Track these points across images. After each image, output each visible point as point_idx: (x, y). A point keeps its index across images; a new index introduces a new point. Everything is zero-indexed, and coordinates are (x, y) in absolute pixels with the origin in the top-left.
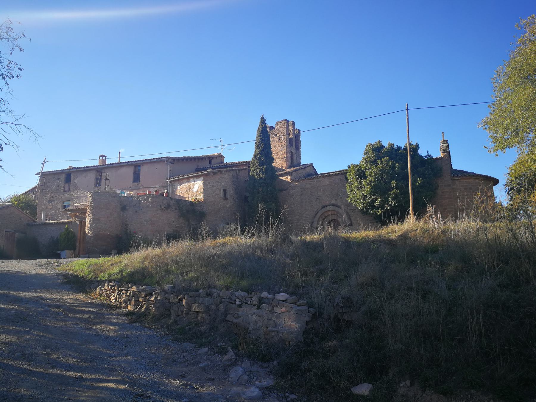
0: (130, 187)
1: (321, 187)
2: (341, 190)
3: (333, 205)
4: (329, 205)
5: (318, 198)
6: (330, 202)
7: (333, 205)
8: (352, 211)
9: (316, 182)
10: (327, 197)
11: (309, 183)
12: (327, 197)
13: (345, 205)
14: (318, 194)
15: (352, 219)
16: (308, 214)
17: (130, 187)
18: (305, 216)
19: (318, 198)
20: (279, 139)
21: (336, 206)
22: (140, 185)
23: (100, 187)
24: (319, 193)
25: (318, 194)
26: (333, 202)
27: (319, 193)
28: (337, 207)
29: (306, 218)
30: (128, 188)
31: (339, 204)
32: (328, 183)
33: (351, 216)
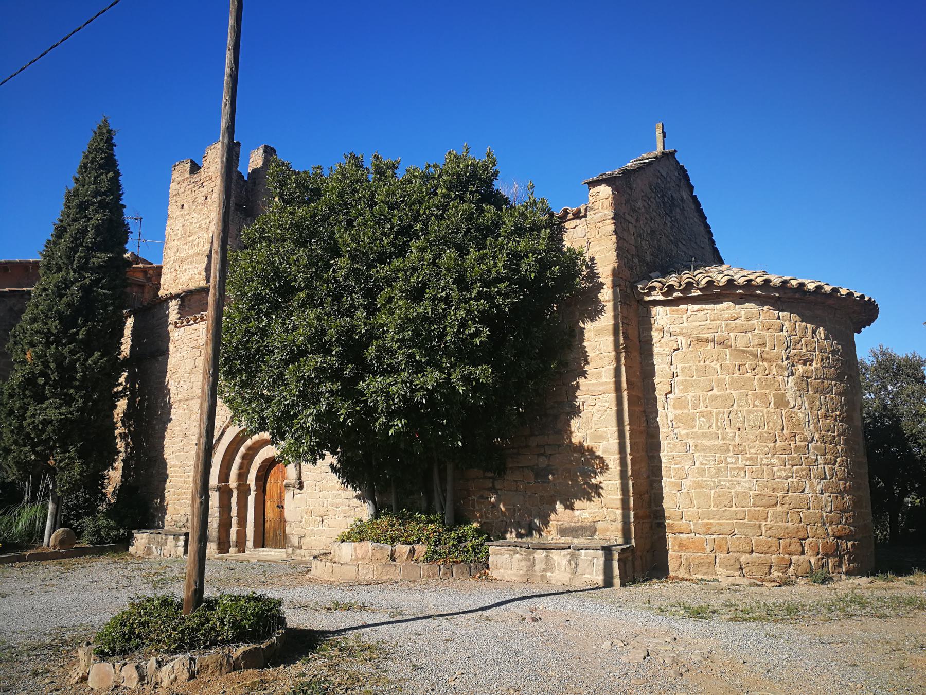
20: (206, 198)
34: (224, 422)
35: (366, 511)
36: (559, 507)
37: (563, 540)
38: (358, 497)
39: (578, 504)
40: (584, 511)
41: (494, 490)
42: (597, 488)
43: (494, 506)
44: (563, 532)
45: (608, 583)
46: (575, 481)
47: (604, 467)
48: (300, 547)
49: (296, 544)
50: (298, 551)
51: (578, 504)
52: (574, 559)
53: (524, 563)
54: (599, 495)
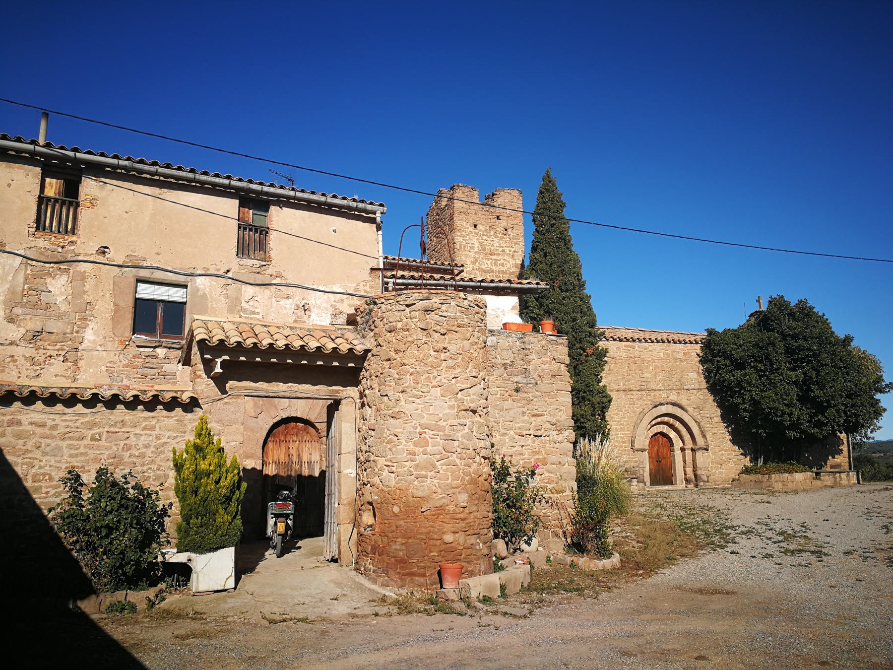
0: (228, 271)
1: (650, 361)
2: (688, 375)
3: (674, 404)
4: (667, 404)
5: (644, 384)
6: (668, 397)
7: (674, 404)
8: (707, 419)
9: (638, 349)
10: (661, 385)
11: (624, 348)
12: (661, 385)
13: (695, 407)
14: (644, 375)
15: (707, 437)
16: (624, 418)
17: (228, 271)
18: (618, 421)
19: (644, 384)
20: (506, 230)
21: (679, 407)
22: (271, 270)
23: (74, 238)
24: (646, 375)
25: (644, 375)
26: (673, 397)
27: (646, 375)
28: (679, 409)
29: (621, 424)
30: (219, 270)
31: (684, 403)
32: (662, 355)
33: (706, 429)
34: (644, 410)
35: (747, 461)
36: (830, 457)
37: (831, 470)
38: (742, 454)
39: (836, 456)
40: (839, 459)
41: (808, 452)
42: (842, 450)
43: (808, 458)
44: (832, 467)
45: (859, 483)
46: (835, 448)
47: (843, 444)
48: (708, 482)
49: (706, 480)
50: (707, 483)
51: (836, 456)
52: (848, 475)
53: (833, 479)
54: (842, 453)
